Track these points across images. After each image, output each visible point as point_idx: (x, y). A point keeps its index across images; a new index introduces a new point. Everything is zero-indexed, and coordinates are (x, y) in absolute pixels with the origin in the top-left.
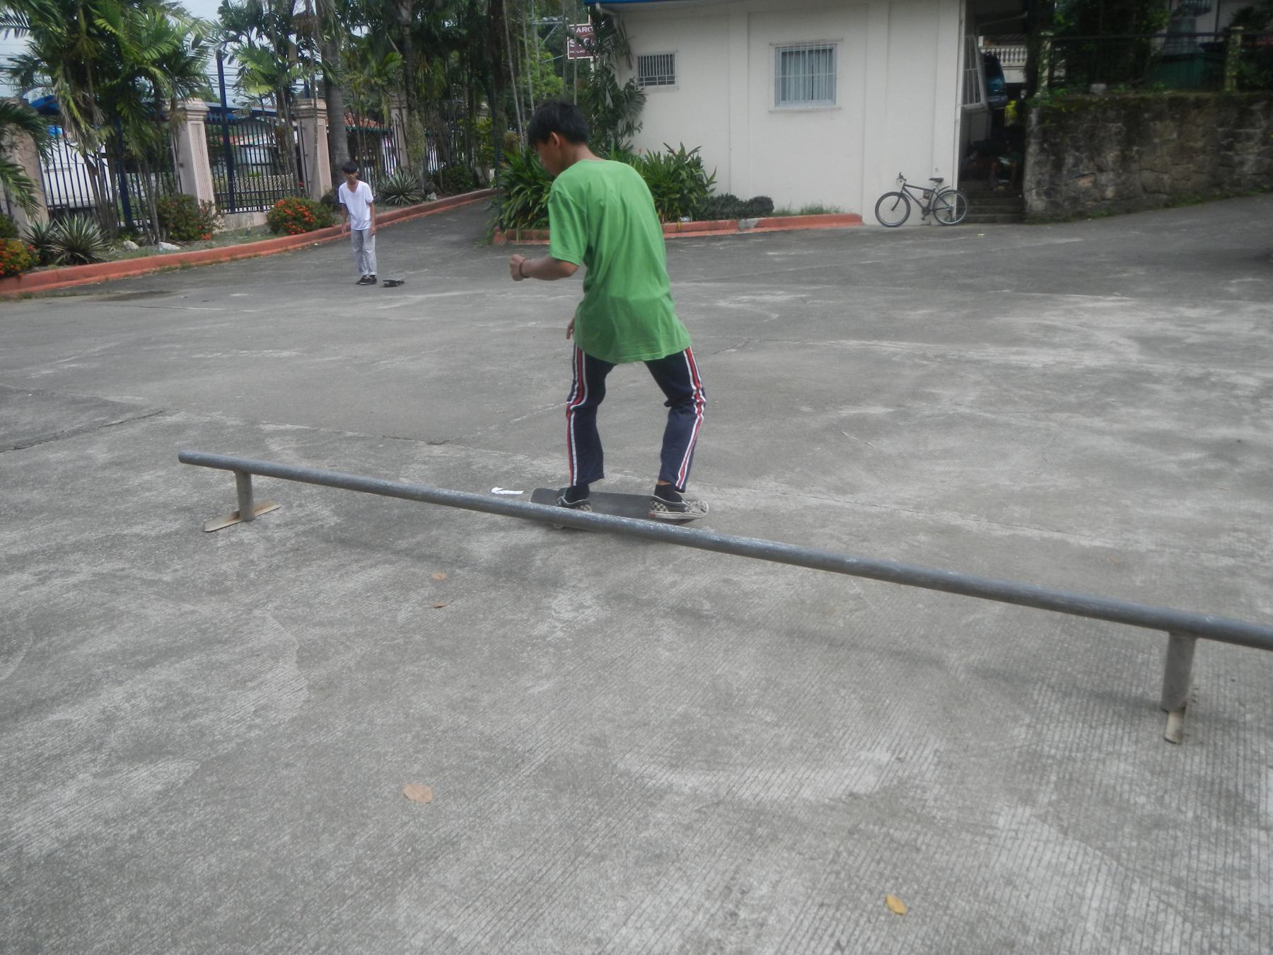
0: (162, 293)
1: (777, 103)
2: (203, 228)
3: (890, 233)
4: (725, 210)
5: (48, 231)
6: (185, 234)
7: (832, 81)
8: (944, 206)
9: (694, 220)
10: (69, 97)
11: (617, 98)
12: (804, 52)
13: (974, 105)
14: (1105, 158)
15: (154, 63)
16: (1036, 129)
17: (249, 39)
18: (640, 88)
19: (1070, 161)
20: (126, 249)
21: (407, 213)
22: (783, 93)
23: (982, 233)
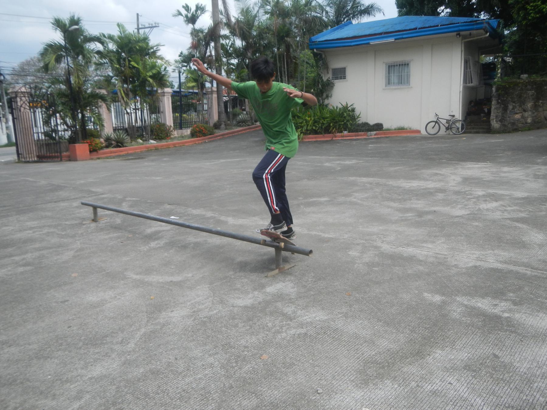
0: (142, 158)
1: (386, 86)
2: (167, 135)
3: (430, 138)
4: (363, 129)
5: (111, 135)
6: (160, 137)
7: (408, 76)
8: (455, 126)
9: (349, 132)
10: (121, 90)
11: (323, 86)
12: (397, 65)
13: (471, 85)
14: (527, 106)
15: (151, 77)
16: (495, 94)
17: (190, 67)
18: (332, 81)
19: (510, 107)
20: (137, 142)
21: (245, 130)
22: (389, 82)
23: (465, 137)
